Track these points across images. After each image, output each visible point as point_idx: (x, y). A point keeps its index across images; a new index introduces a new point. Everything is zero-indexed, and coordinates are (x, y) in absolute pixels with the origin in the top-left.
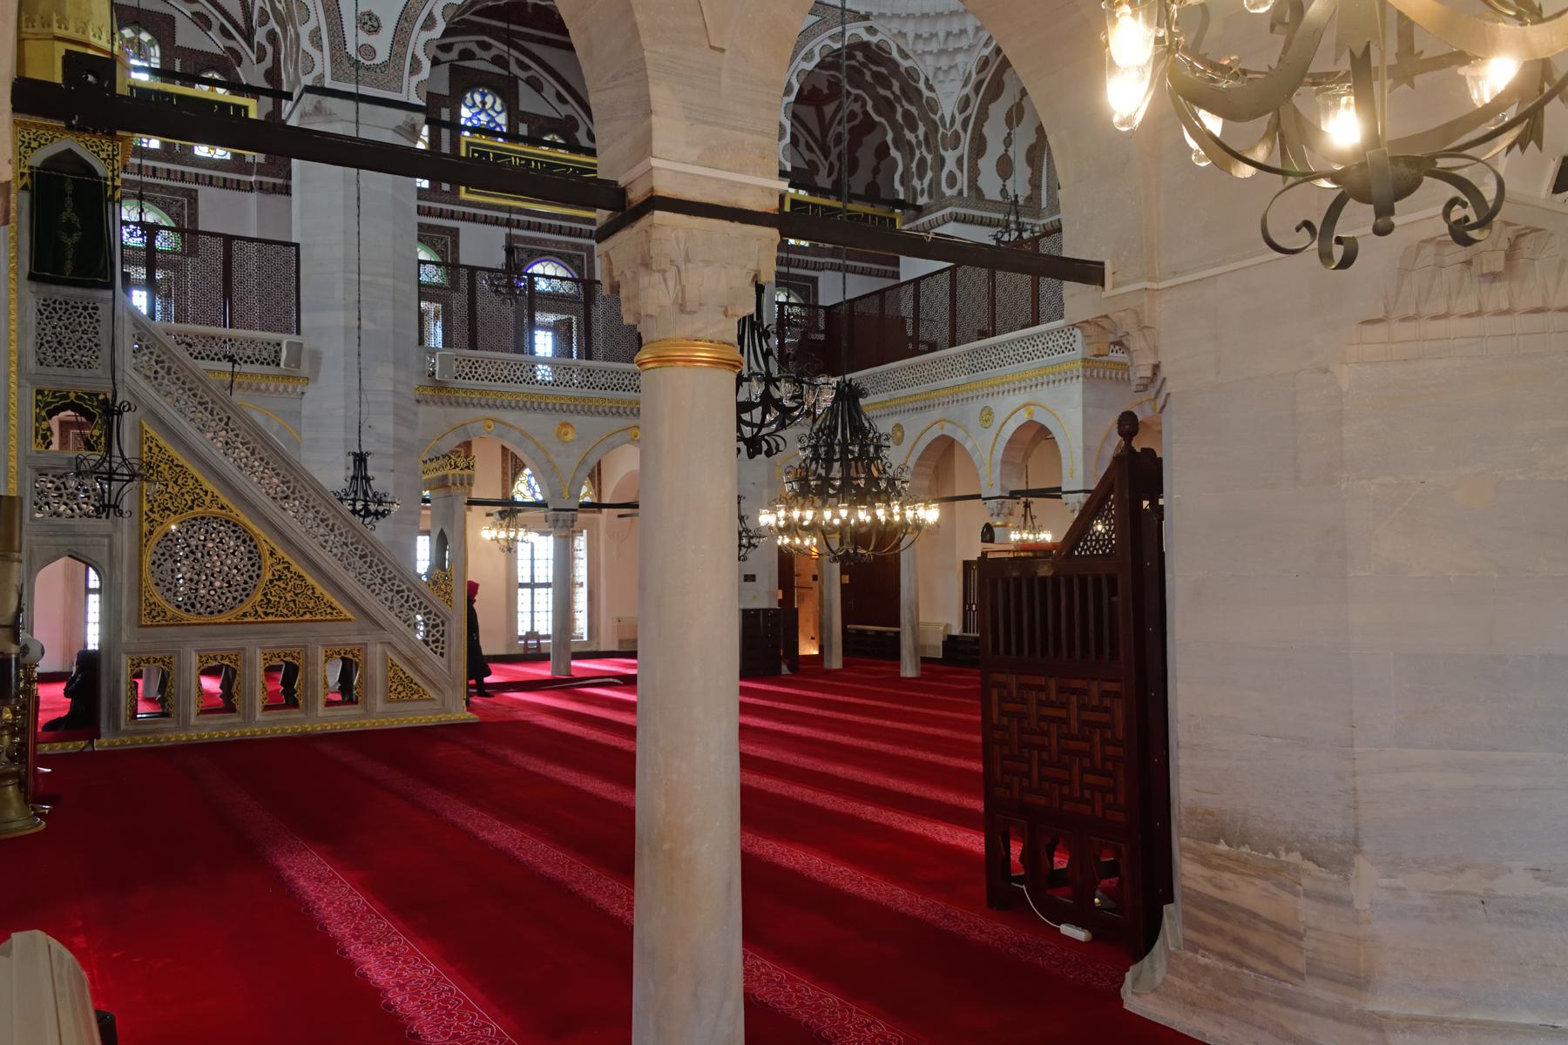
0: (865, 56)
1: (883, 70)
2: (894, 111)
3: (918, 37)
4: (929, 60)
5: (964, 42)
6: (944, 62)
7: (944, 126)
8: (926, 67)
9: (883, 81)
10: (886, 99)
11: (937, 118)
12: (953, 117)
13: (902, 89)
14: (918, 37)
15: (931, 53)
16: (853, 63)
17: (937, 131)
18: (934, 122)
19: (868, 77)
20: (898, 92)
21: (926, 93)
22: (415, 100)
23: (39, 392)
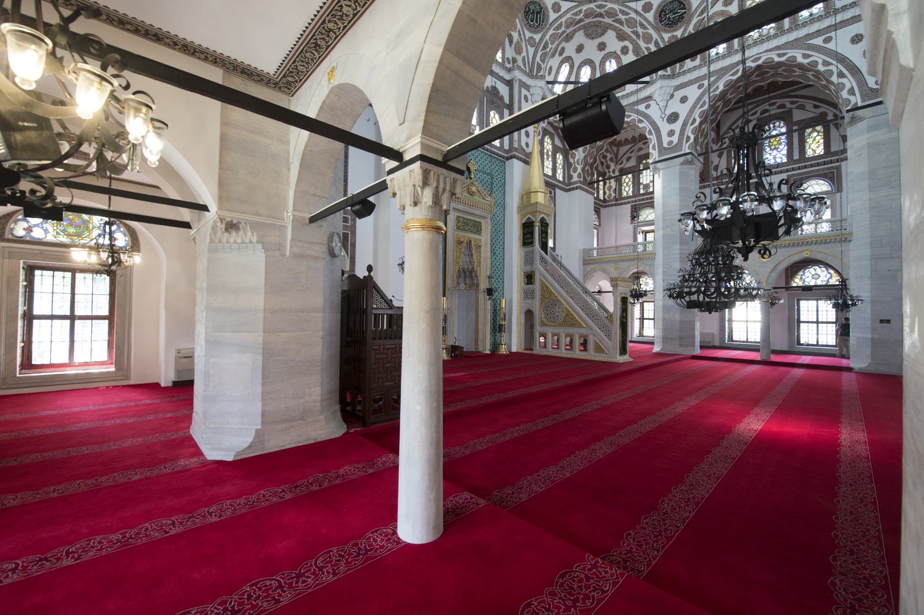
22: (688, 151)
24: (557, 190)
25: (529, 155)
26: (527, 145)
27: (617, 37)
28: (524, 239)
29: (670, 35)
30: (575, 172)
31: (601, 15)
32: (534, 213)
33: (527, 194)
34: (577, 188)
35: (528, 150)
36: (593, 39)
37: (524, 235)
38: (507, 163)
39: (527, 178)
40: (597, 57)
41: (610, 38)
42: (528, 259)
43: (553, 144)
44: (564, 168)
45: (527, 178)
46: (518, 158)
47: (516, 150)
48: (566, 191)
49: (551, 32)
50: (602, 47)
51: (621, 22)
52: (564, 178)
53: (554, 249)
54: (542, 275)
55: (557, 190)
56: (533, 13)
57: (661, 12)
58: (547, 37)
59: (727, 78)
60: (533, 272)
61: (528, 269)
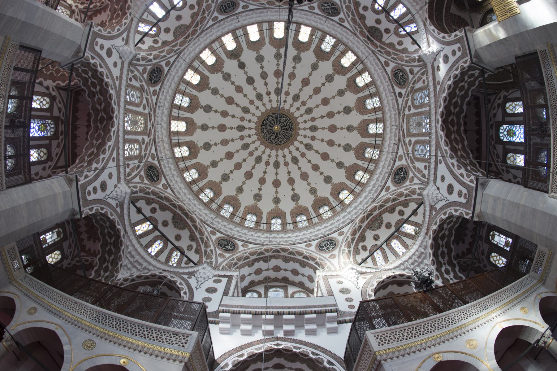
0: (114, 242)
1: (114, 250)
2: (104, 263)
3: (130, 253)
4: (127, 261)
5: (139, 267)
6: (129, 266)
7: (116, 278)
8: (125, 262)
9: (110, 253)
10: (105, 258)
11: (116, 274)
12: (120, 279)
13: (113, 260)
14: (130, 253)
15: (129, 260)
16: (109, 240)
17: (113, 277)
18: (114, 275)
19: (107, 249)
20: (111, 259)
21: (119, 266)
27: (166, 41)
29: (148, 70)
31: (186, 38)
36: (177, 28)
40: (163, 25)
41: (169, 37)
49: (212, 9)
50: (167, 30)
51: (174, 46)
56: (229, 7)
57: (160, 70)
58: (214, 5)
59: (114, 97)
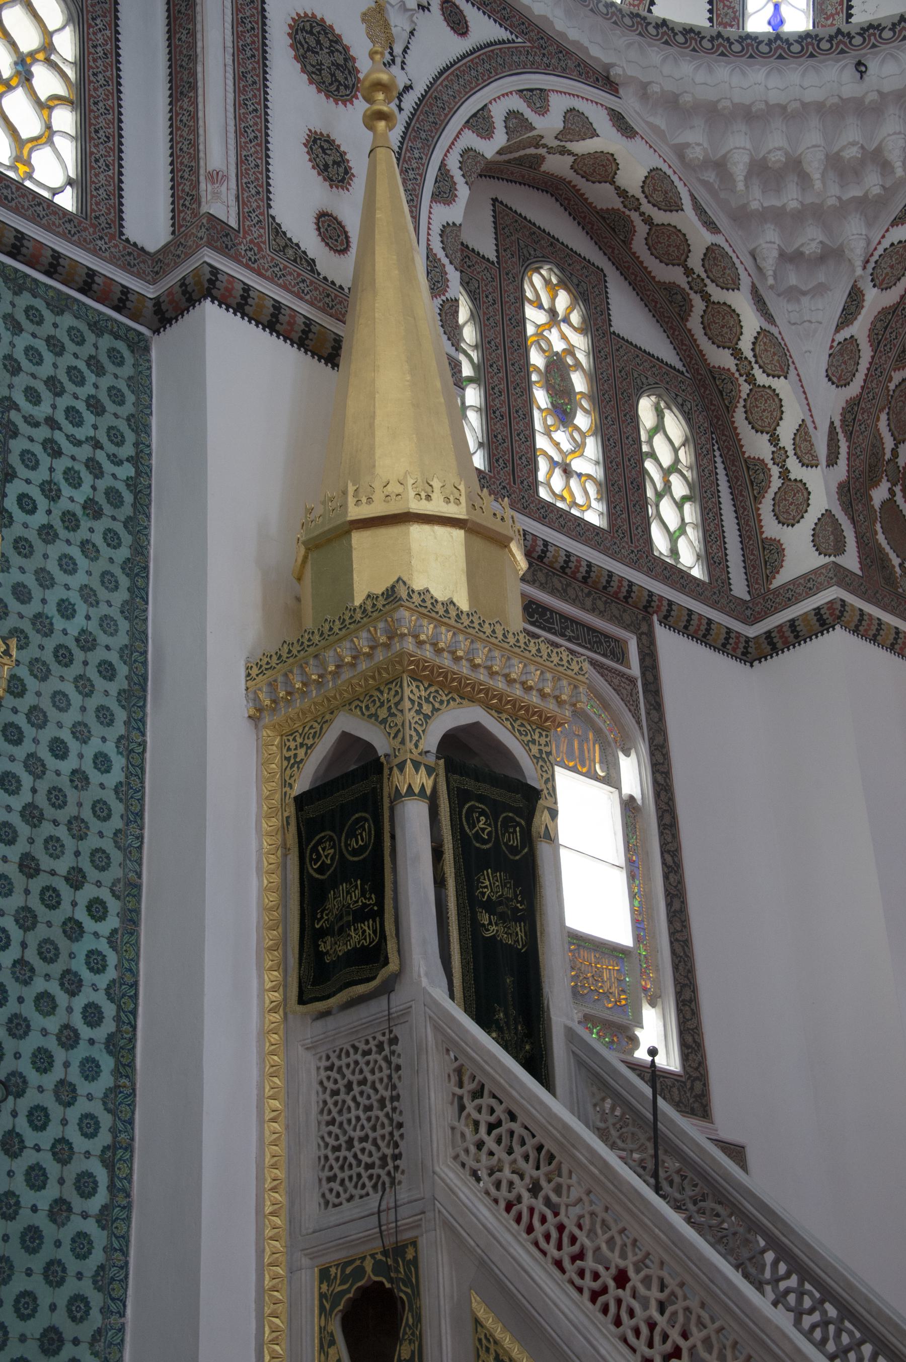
23: (324, 1275)
24: (670, 644)
25: (337, 300)
26: (331, 229)
28: (311, 935)
30: (788, 519)
32: (376, 693)
33: (327, 542)
34: (823, 621)
35: (336, 268)
37: (313, 894)
38: (162, 348)
39: (328, 446)
42: (356, 1136)
43: (597, 325)
44: (703, 492)
45: (328, 446)
46: (242, 304)
47: (221, 236)
48: (750, 653)
52: (713, 553)
53: (691, 1088)
54: (488, 1277)
55: (670, 644)
60: (400, 1255)
61: (355, 1225)
